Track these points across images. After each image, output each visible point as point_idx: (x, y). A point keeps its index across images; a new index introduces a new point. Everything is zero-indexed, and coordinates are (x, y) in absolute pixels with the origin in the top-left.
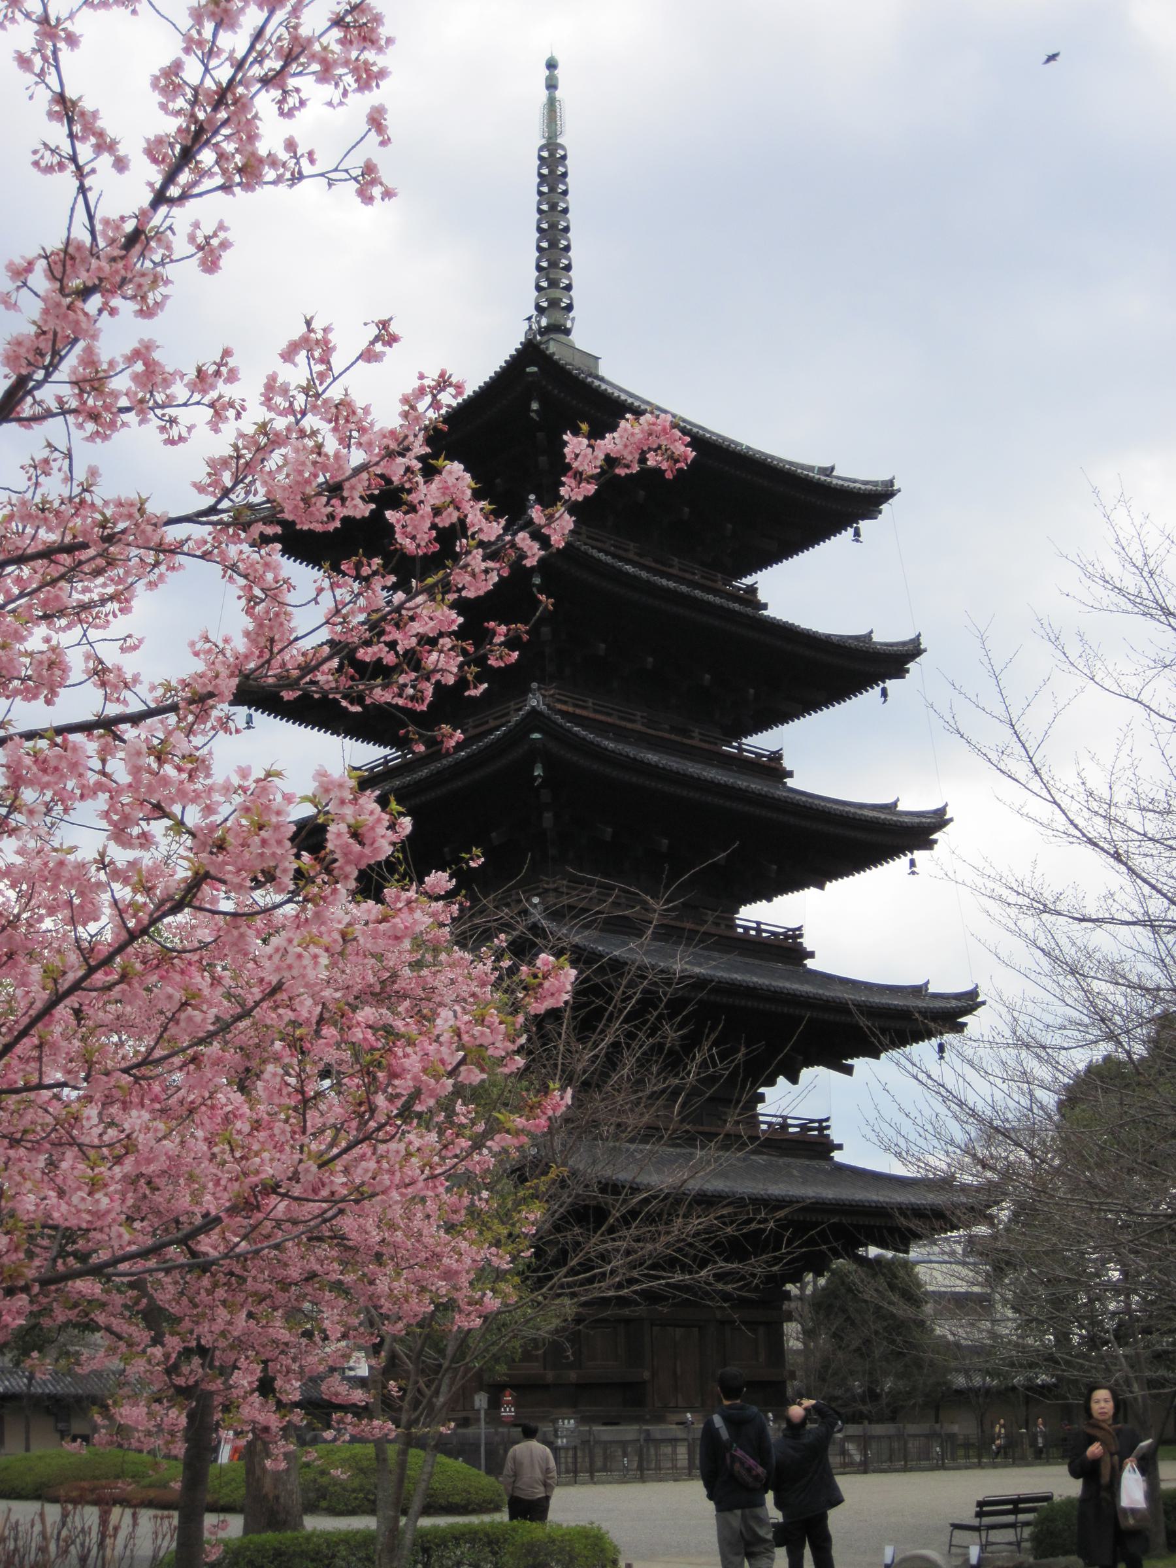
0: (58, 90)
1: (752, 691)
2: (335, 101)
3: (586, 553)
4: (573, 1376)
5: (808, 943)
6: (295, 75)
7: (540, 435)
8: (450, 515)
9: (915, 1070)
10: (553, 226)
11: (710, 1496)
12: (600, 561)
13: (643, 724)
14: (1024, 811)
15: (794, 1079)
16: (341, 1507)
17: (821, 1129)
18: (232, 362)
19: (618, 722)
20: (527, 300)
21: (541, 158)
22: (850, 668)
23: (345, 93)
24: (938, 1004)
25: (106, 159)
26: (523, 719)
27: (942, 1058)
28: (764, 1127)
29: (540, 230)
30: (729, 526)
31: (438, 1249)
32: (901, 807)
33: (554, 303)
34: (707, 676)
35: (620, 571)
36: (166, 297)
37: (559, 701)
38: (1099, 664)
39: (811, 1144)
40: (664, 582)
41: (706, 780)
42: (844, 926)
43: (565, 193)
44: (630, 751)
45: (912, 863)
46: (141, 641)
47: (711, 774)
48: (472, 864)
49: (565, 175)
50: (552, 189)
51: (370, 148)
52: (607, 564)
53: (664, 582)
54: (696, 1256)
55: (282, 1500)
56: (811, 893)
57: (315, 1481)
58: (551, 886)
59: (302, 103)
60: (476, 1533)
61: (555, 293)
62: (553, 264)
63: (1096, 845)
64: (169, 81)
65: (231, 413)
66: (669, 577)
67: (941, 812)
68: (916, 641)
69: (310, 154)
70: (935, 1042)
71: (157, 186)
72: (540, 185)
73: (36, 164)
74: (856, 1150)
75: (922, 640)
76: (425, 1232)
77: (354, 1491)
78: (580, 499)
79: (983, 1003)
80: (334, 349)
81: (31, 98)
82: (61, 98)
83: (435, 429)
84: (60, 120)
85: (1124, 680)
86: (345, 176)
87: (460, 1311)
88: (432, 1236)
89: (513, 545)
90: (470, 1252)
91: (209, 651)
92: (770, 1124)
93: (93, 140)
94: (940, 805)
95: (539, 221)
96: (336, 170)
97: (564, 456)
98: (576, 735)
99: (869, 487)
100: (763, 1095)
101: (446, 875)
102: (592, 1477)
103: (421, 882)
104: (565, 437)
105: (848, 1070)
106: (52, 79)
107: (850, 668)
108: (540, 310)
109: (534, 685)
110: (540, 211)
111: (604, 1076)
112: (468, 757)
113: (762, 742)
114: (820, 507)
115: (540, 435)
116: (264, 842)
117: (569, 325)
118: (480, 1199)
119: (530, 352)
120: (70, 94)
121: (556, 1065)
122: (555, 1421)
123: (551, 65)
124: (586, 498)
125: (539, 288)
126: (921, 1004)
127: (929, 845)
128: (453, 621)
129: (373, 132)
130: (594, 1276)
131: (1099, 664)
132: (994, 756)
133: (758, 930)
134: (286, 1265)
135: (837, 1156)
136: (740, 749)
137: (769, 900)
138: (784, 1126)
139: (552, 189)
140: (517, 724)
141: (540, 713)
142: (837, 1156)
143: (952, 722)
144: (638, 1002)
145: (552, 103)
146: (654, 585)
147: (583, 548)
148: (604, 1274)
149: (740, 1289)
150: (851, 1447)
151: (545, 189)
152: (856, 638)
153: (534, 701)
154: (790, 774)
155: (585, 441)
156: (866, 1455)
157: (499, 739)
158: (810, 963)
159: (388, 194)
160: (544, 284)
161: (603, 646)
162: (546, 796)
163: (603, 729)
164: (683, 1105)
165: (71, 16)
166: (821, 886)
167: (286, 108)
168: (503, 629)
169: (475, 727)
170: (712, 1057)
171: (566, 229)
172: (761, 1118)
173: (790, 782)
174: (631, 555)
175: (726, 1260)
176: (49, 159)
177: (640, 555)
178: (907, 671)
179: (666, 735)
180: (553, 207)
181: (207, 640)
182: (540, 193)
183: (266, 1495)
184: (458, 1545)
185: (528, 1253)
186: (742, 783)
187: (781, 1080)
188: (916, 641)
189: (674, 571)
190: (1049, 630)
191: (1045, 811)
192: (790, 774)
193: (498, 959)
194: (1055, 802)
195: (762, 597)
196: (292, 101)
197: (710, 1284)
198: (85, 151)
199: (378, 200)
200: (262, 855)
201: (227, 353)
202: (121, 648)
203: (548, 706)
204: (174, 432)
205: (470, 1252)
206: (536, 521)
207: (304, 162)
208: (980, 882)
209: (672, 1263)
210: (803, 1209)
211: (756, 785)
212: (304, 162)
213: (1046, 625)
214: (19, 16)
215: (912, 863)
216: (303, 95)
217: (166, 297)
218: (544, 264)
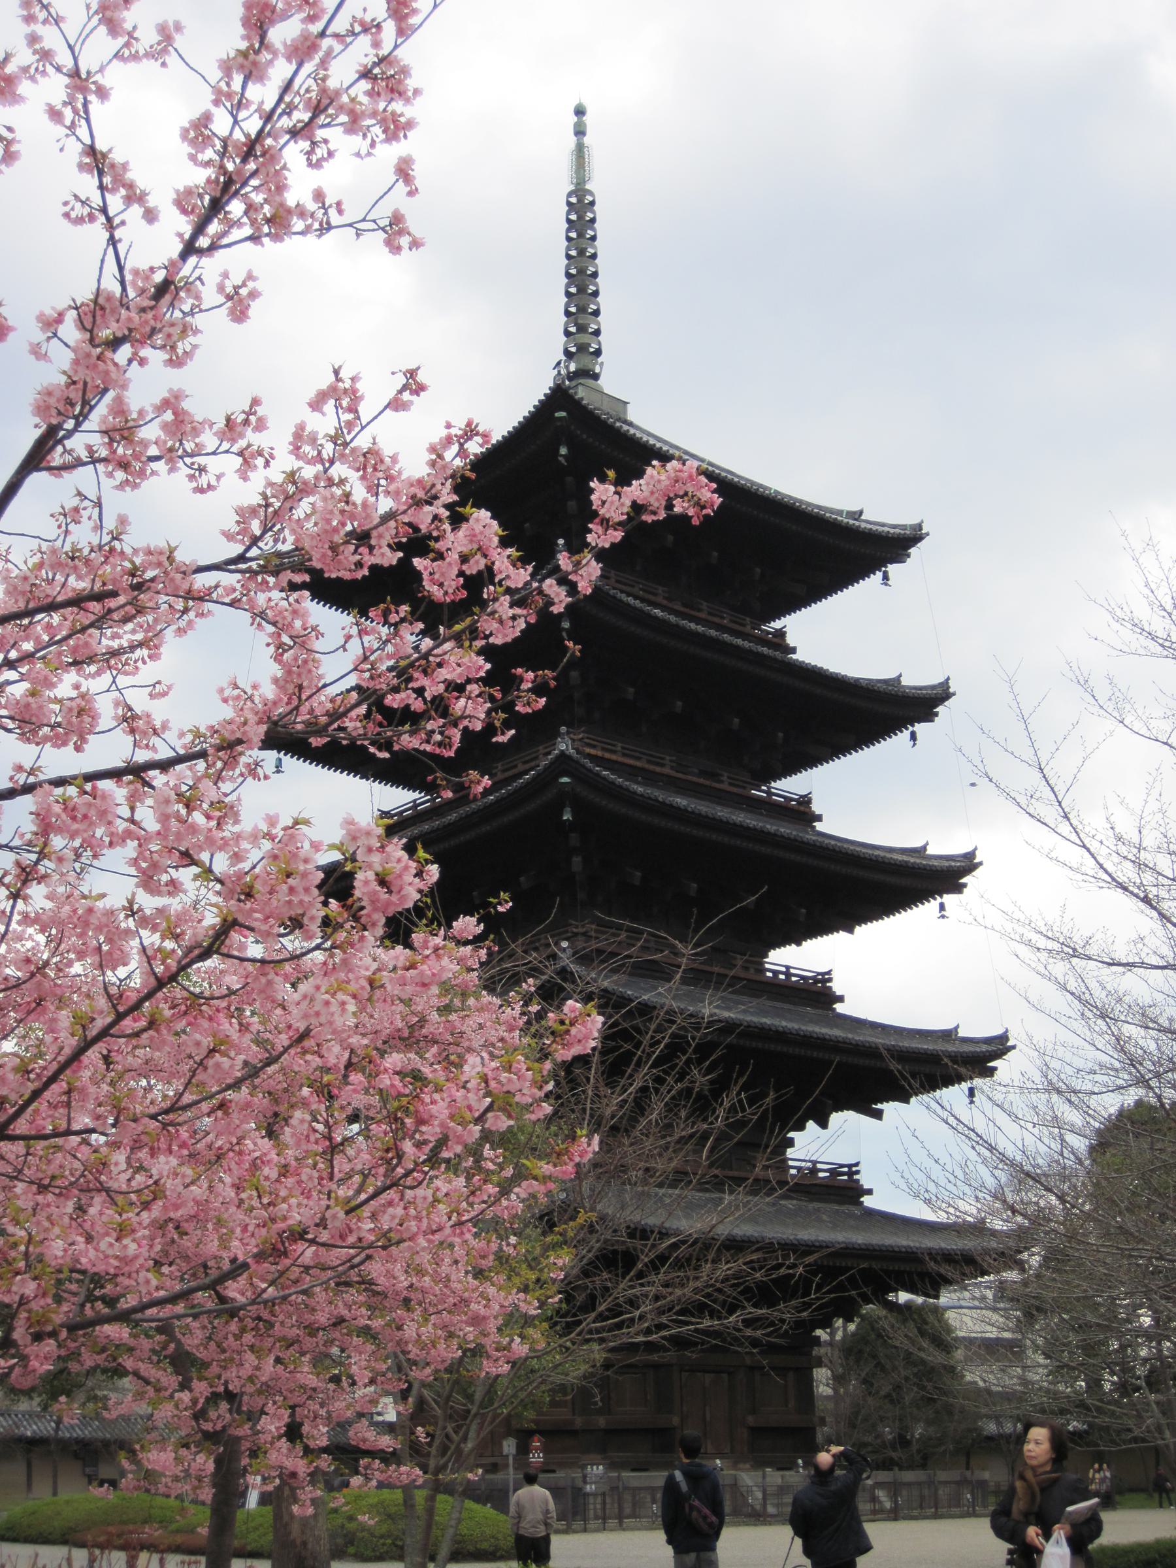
0: (88, 142)
1: (781, 735)
2: (363, 152)
3: (614, 597)
4: (601, 1422)
5: (837, 987)
6: (323, 126)
7: (569, 479)
8: (477, 562)
9: (945, 1115)
10: (582, 271)
11: (669, 1542)
12: (628, 605)
13: (672, 768)
14: (1053, 855)
15: (823, 1124)
16: (369, 1553)
17: (851, 1174)
18: (260, 411)
19: (647, 766)
20: (555, 345)
21: (569, 204)
22: (878, 712)
23: (373, 144)
25: (136, 210)
26: (552, 763)
27: (972, 1102)
28: (793, 1171)
29: (568, 275)
30: (758, 570)
32: (931, 851)
33: (583, 348)
34: (736, 720)
35: (649, 615)
36: (195, 347)
38: (1128, 707)
39: (841, 1189)
40: (693, 626)
41: (735, 824)
42: (873, 971)
43: (594, 238)
44: (660, 795)
45: (942, 907)
46: (170, 687)
48: (500, 909)
49: (593, 220)
50: (581, 235)
51: (398, 198)
52: (635, 608)
53: (693, 626)
54: (725, 1302)
55: (310, 1546)
56: (841, 936)
57: (343, 1526)
58: (581, 930)
59: (331, 154)
61: (583, 338)
62: (582, 309)
63: (1125, 889)
64: (198, 132)
65: (260, 462)
66: (698, 621)
67: (971, 855)
69: (339, 204)
70: (965, 1086)
71: (187, 236)
72: (568, 230)
73: (67, 215)
74: (884, 1197)
75: (951, 683)
76: (453, 1278)
77: (382, 1537)
78: (607, 545)
79: (1014, 1047)
80: (362, 398)
81: (61, 150)
82: (91, 150)
83: (463, 477)
84: (90, 171)
85: (1153, 723)
86: (373, 226)
87: (489, 1357)
88: (460, 1282)
89: (540, 591)
90: (497, 1298)
91: (238, 698)
92: (799, 1169)
93: (123, 192)
94: (969, 849)
95: (568, 267)
96: (364, 220)
97: (591, 503)
98: (604, 778)
99: (897, 531)
100: (792, 1139)
101: (474, 920)
102: (621, 1523)
103: (450, 927)
104: (592, 484)
105: (878, 1115)
106: (83, 132)
107: (878, 712)
108: (569, 355)
109: (563, 729)
110: (568, 257)
111: (633, 1121)
112: (497, 801)
113: (791, 786)
114: (847, 552)
115: (569, 479)
116: (292, 890)
117: (597, 370)
118: (508, 1244)
119: (559, 397)
120: (101, 146)
121: (584, 1110)
122: (584, 1467)
123: (580, 112)
124: (613, 544)
125: (567, 333)
126: (951, 1048)
127: (958, 888)
128: (481, 667)
129: (401, 183)
130: (623, 1322)
131: (1128, 707)
132: (1023, 800)
133: (788, 974)
134: (314, 1310)
135: (867, 1201)
136: (769, 793)
137: (799, 944)
138: (814, 1171)
139: (581, 235)
140: (546, 768)
141: (569, 757)
142: (867, 1201)
143: (981, 766)
144: (666, 1046)
145: (580, 150)
146: (684, 629)
147: (612, 592)
148: (632, 1320)
149: (768, 1335)
150: (881, 1494)
151: (573, 235)
152: (885, 681)
153: (564, 745)
154: (819, 818)
155: (612, 488)
156: (896, 1502)
157: (528, 783)
158: (839, 1008)
159: (415, 244)
160: (573, 329)
161: (631, 690)
162: (574, 839)
163: (632, 773)
164: (712, 1150)
165: (101, 70)
166: (851, 931)
167: (314, 159)
168: (531, 675)
169: (504, 771)
170: (740, 1101)
171: (595, 275)
172: (791, 1163)
173: (819, 826)
174: (659, 600)
175: (755, 1306)
176: (79, 210)
177: (669, 599)
178: (936, 714)
179: (695, 779)
180: (582, 252)
181: (236, 687)
182: (569, 239)
183: (294, 1541)
185: (556, 1299)
186: (771, 827)
187: (811, 1124)
189: (703, 615)
190: (1078, 673)
191: (1075, 855)
192: (819, 818)
193: (526, 1004)
194: (1084, 846)
195: (791, 640)
196: (320, 152)
197: (739, 1330)
198: (115, 202)
199: (405, 251)
200: (290, 902)
201: (255, 402)
202: (151, 695)
203: (577, 750)
204: (204, 481)
205: (497, 1298)
206: (563, 567)
207: (333, 212)
208: (1009, 927)
209: (701, 1309)
210: (831, 1255)
211: (785, 829)
212: (333, 212)
213: (1075, 668)
214: (49, 69)
215: (942, 907)
216: (332, 146)
217: (195, 347)
218: (573, 310)
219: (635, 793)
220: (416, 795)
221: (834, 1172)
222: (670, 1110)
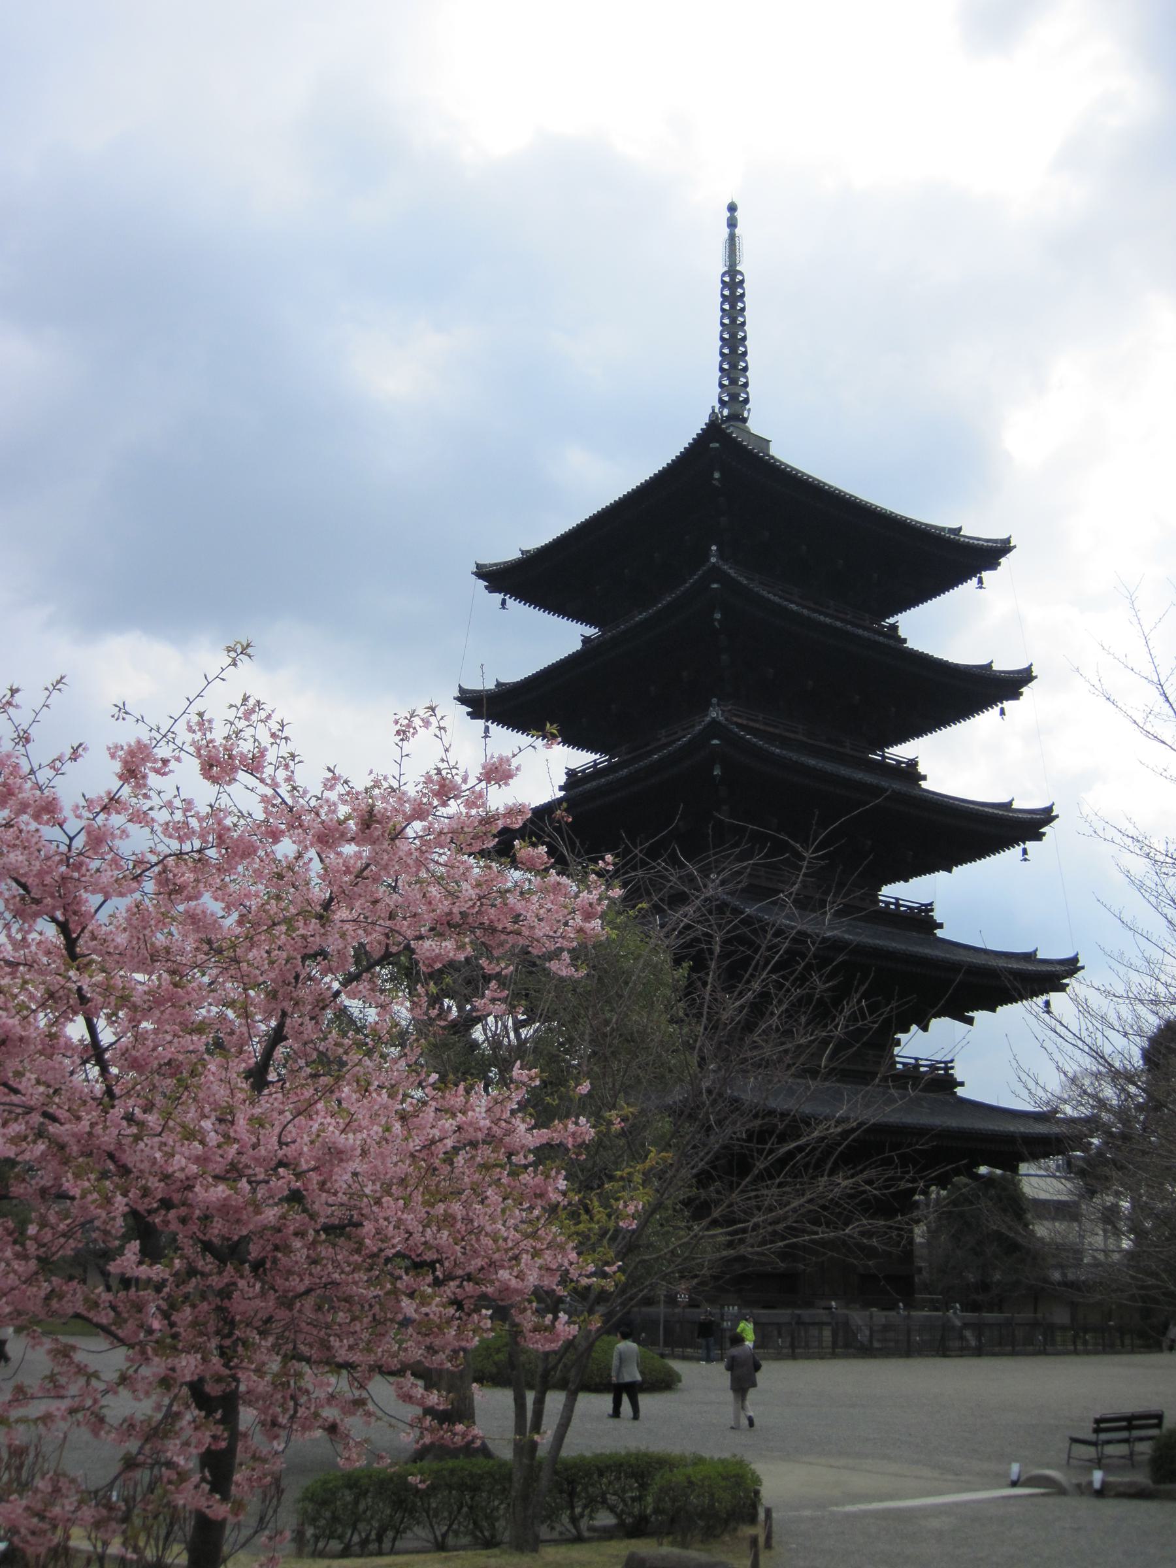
5: (938, 916)
10: (733, 335)
12: (769, 600)
15: (925, 1029)
17: (947, 1069)
21: (723, 282)
24: (1044, 968)
26: (704, 729)
28: (899, 1066)
29: (722, 339)
31: (496, 1256)
32: (1015, 806)
33: (734, 397)
37: (736, 715)
39: (940, 1081)
40: (822, 618)
42: (966, 902)
43: (743, 309)
45: (1025, 852)
47: (859, 775)
49: (743, 295)
50: (733, 306)
53: (822, 618)
54: (840, 1213)
56: (942, 875)
60: (621, 1465)
62: (734, 366)
66: (826, 615)
67: (1049, 809)
68: (1028, 670)
70: (1040, 1000)
72: (722, 303)
79: (1083, 968)
92: (904, 1064)
94: (1048, 805)
98: (748, 741)
105: (970, 1021)
108: (721, 401)
109: (714, 700)
110: (722, 324)
112: (660, 760)
113: (902, 751)
117: (746, 415)
119: (714, 431)
122: (722, 1307)
125: (721, 385)
126: (1031, 967)
127: (1039, 837)
133: (897, 905)
134: (290, 1272)
135: (960, 1091)
137: (906, 881)
138: (917, 1066)
139: (733, 306)
141: (719, 723)
142: (960, 1091)
144: (786, 952)
148: (744, 1231)
150: (968, 1334)
151: (727, 307)
154: (924, 778)
158: (939, 933)
160: (726, 383)
166: (950, 871)
172: (898, 1059)
173: (924, 784)
175: (872, 1217)
178: (1021, 694)
180: (733, 320)
182: (723, 310)
184: (601, 1475)
185: (614, 1268)
187: (914, 1028)
188: (1028, 670)
192: (924, 778)
195: (902, 633)
203: (727, 719)
209: (816, 1222)
211: (897, 786)
215: (1025, 852)
218: (726, 367)
219: (773, 753)
220: (598, 756)
221: (933, 1067)
222: (790, 1016)
